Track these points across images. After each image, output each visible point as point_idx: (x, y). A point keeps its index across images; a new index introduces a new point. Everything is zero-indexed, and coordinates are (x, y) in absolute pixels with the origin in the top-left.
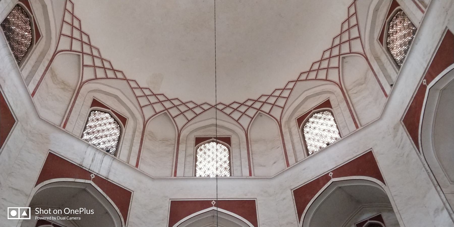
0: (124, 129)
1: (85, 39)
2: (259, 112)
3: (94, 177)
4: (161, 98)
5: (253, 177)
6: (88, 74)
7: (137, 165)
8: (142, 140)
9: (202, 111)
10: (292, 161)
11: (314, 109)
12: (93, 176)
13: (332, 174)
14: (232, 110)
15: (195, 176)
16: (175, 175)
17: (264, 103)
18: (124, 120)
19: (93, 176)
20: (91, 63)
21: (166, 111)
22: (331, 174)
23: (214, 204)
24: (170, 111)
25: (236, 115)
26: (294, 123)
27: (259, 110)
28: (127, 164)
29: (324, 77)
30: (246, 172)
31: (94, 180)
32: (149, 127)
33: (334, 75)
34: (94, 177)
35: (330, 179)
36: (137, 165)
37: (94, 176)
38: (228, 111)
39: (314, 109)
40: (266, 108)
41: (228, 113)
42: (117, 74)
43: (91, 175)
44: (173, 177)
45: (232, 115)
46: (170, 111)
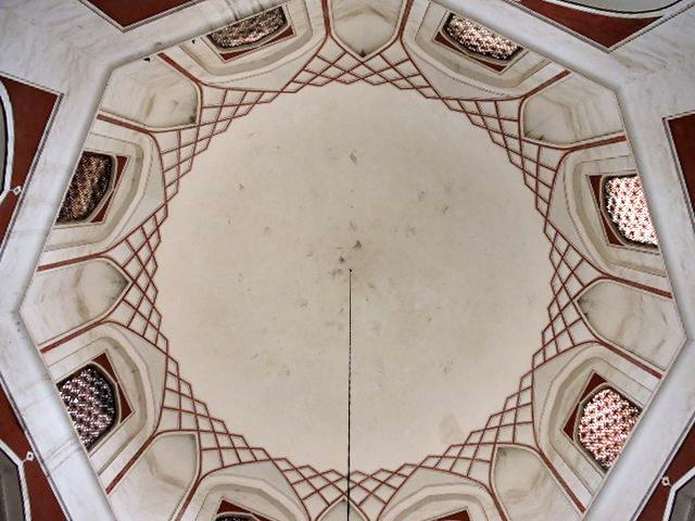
1: (150, 268)
3: (31, 459)
4: (199, 410)
6: (122, 314)
7: (109, 489)
8: (135, 458)
9: (251, 459)
12: (30, 457)
14: (300, 478)
18: (127, 411)
19: (30, 457)
20: (134, 302)
25: (304, 490)
28: (96, 475)
29: (464, 472)
31: (27, 465)
32: (157, 446)
33: (480, 472)
34: (31, 459)
36: (109, 489)
38: (293, 477)
41: (292, 481)
42: (157, 340)
43: (29, 453)
45: (297, 487)
46: (203, 435)
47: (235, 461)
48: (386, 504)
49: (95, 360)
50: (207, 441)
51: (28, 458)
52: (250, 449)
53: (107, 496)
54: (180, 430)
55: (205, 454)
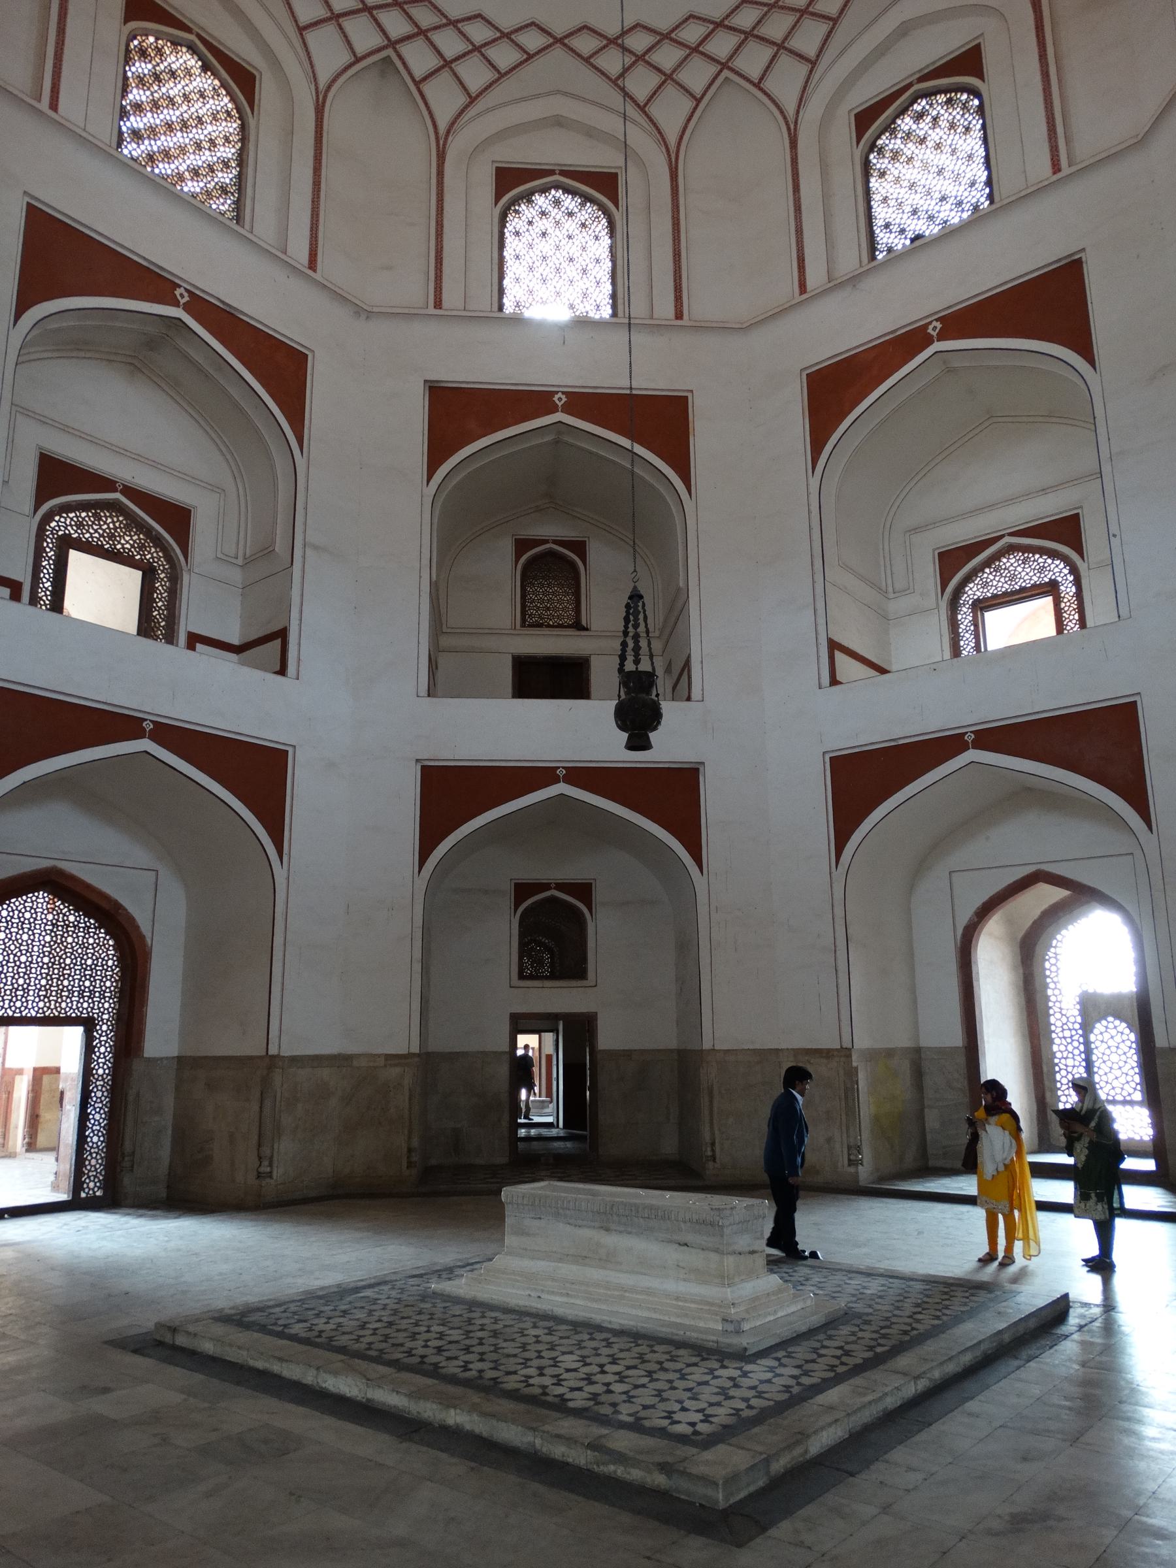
0: (252, 122)
2: (726, 73)
3: (186, 299)
5: (685, 322)
7: (312, 264)
10: (816, 277)
11: (921, 80)
13: (939, 325)
15: (501, 307)
16: (438, 304)
17: (749, 35)
21: (389, 52)
22: (935, 328)
23: (560, 404)
24: (406, 50)
25: (641, 83)
26: (844, 128)
27: (724, 66)
30: (665, 308)
31: (187, 308)
34: (186, 299)
35: (929, 341)
36: (312, 264)
37: (186, 294)
38: (612, 62)
39: (921, 80)
40: (753, 60)
43: (178, 292)
44: (432, 310)
46: (406, 50)
47: (489, 75)
48: (813, 63)
49: (126, 21)
50: (419, 59)
51: (182, 301)
52: (506, 36)
53: (317, 276)
54: (358, 60)
55: (427, 88)
